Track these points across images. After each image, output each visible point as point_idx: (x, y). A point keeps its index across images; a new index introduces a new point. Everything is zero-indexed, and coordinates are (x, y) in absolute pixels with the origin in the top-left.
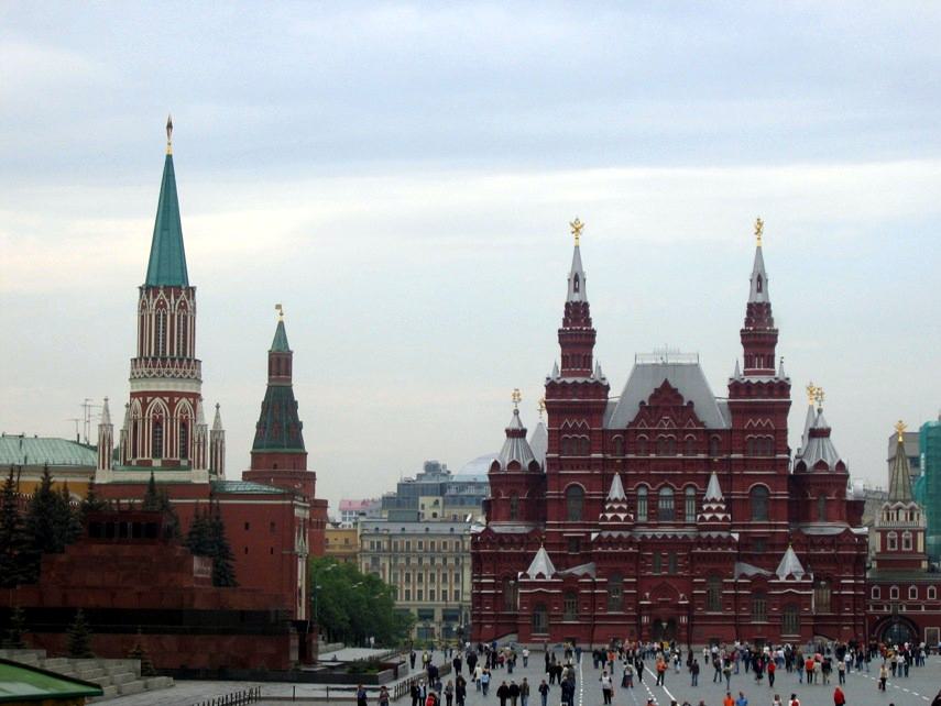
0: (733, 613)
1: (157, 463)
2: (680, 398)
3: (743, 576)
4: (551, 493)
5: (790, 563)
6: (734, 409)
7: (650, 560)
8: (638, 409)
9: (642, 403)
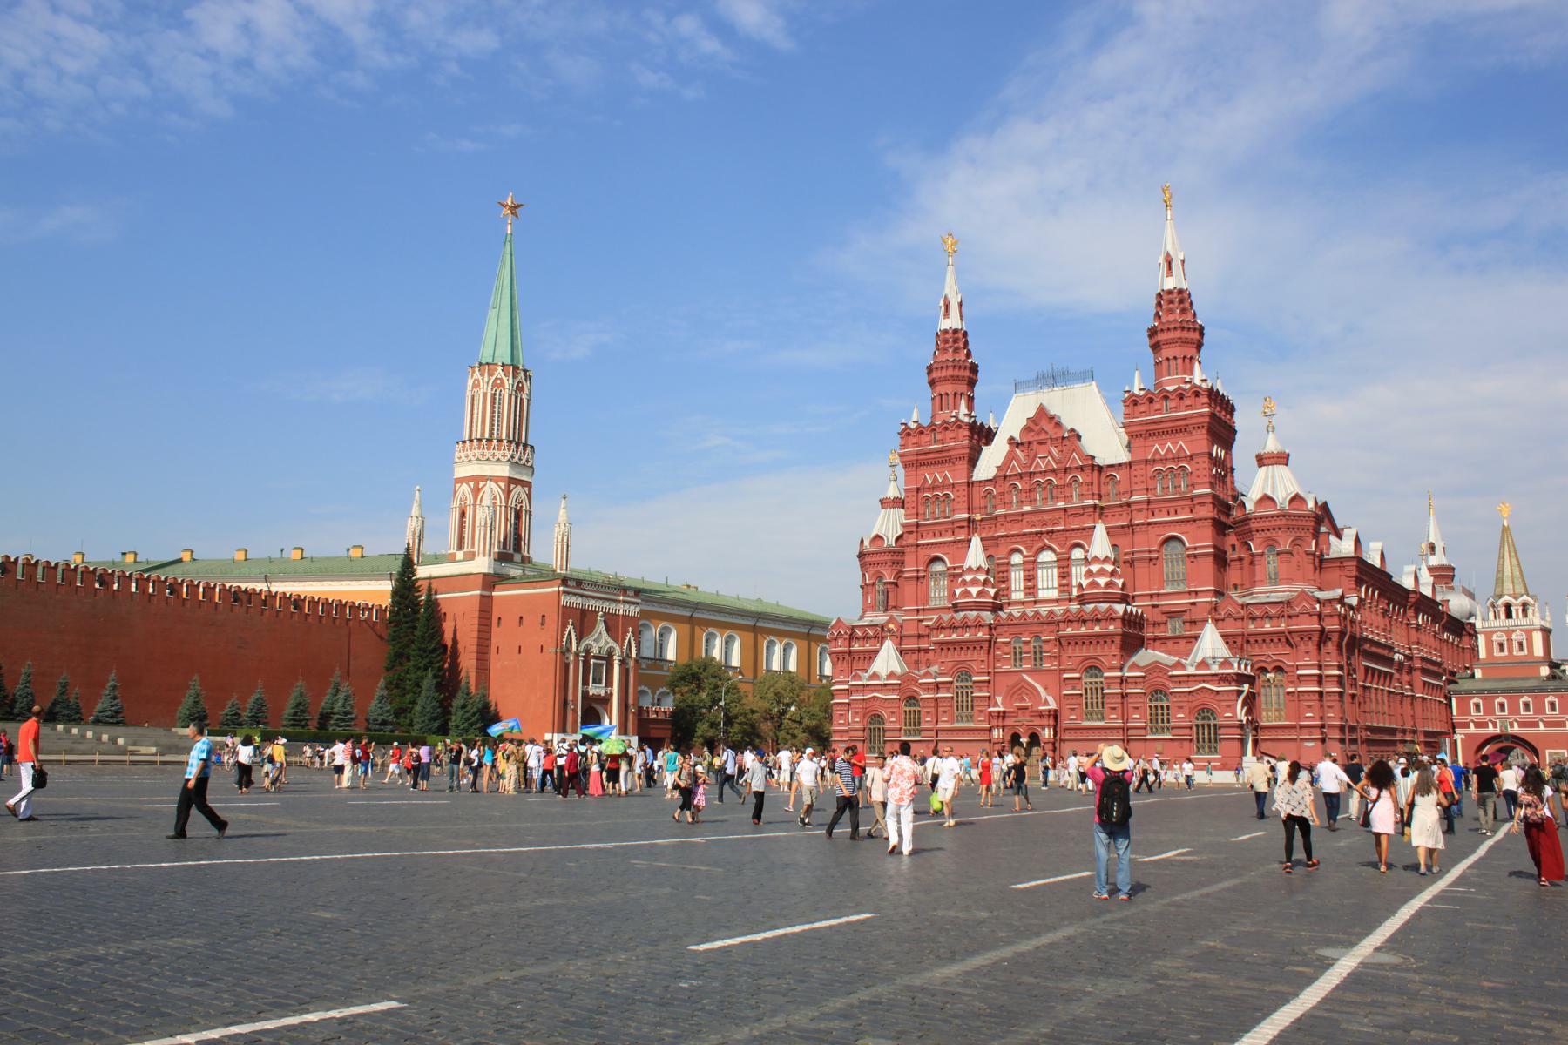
0: (1119, 723)
1: (460, 555)
2: (1058, 425)
3: (1135, 667)
4: (909, 568)
5: (1211, 644)
6: (1137, 435)
7: (1006, 649)
8: (1007, 448)
9: (1012, 438)
